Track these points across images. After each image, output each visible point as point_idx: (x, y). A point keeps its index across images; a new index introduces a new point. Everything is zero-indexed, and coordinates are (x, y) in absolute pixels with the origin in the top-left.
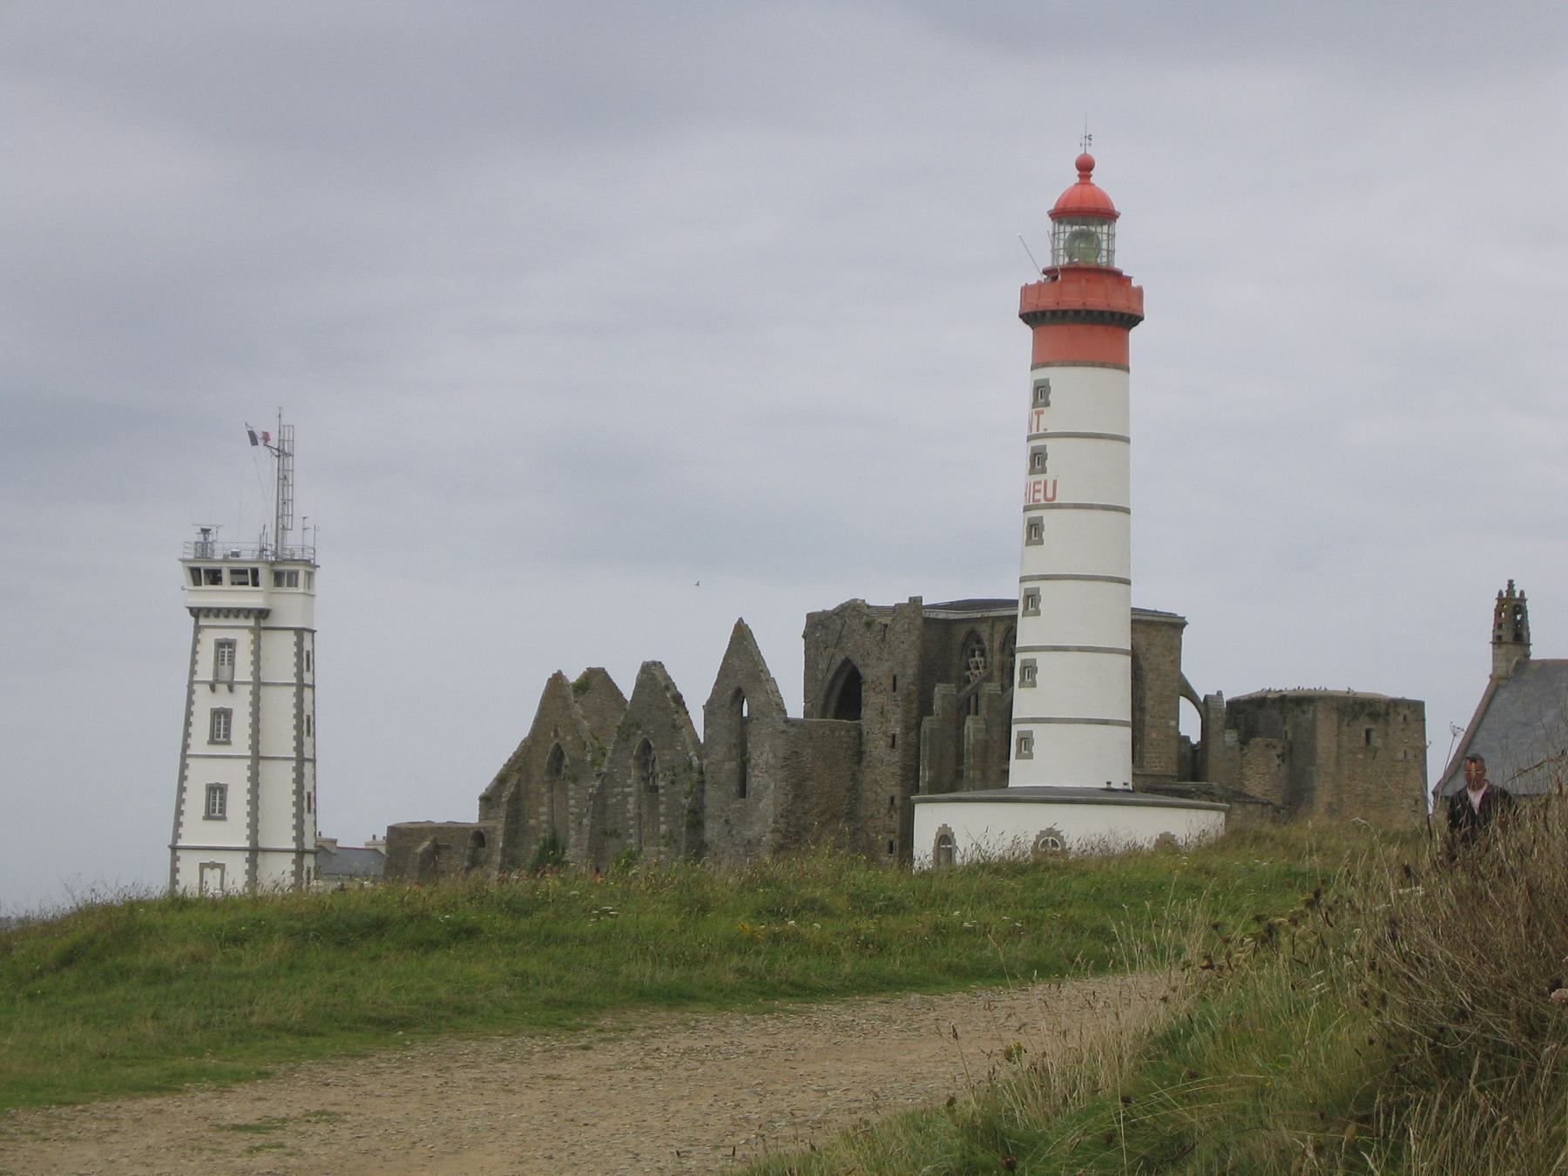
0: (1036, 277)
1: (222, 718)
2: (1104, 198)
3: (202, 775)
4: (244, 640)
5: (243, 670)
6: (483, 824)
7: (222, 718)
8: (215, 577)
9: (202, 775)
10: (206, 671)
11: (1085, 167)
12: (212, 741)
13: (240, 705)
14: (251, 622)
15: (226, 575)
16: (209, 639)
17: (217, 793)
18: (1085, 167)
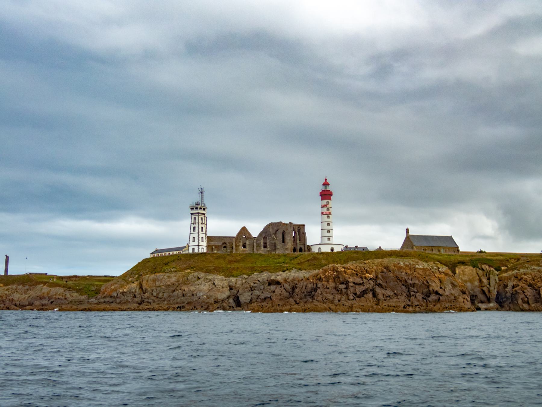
0: (321, 191)
1: (194, 228)
2: (328, 183)
3: (192, 236)
4: (197, 217)
5: (197, 221)
6: (405, 250)
7: (194, 228)
8: (193, 209)
9: (192, 236)
10: (193, 222)
11: (326, 180)
12: (193, 231)
13: (196, 226)
14: (197, 215)
15: (194, 209)
16: (193, 217)
17: (194, 238)
18: (326, 180)
